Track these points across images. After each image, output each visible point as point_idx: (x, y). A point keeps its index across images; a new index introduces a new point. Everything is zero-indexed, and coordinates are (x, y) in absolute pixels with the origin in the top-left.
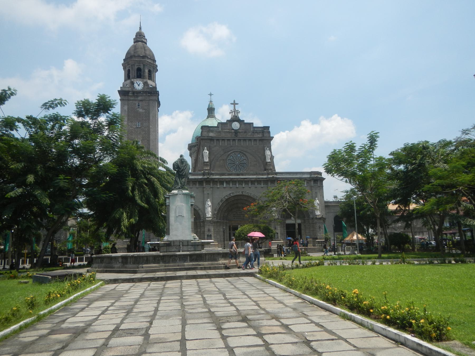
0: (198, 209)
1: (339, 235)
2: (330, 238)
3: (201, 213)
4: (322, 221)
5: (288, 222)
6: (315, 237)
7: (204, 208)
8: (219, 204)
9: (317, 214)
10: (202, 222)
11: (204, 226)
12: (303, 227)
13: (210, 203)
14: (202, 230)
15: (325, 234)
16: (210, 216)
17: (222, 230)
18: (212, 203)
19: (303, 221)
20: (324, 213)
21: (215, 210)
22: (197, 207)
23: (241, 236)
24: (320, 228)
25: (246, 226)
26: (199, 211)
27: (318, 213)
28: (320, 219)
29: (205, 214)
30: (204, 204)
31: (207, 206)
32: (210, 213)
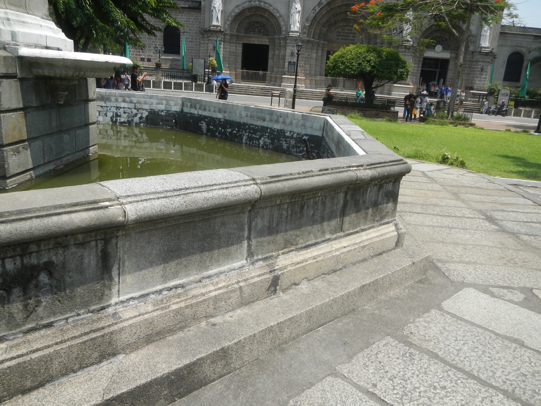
0: (278, 15)
1: (509, 87)
2: (499, 90)
3: (282, 23)
4: (489, 59)
5: (429, 54)
6: (470, 85)
7: (289, 15)
8: (314, 9)
9: (483, 45)
10: (283, 39)
11: (285, 47)
12: (451, 66)
13: (298, 6)
14: (282, 53)
15: (491, 82)
16: (296, 29)
17: (314, 56)
18: (303, 7)
19: (454, 55)
20: (496, 44)
21: (307, 20)
22: (278, 11)
23: (338, 68)
24: (482, 70)
25: (351, 47)
26: (280, 19)
27: (486, 43)
28: (487, 54)
29: (288, 25)
30: (289, 7)
31: (293, 11)
32: (298, 25)
